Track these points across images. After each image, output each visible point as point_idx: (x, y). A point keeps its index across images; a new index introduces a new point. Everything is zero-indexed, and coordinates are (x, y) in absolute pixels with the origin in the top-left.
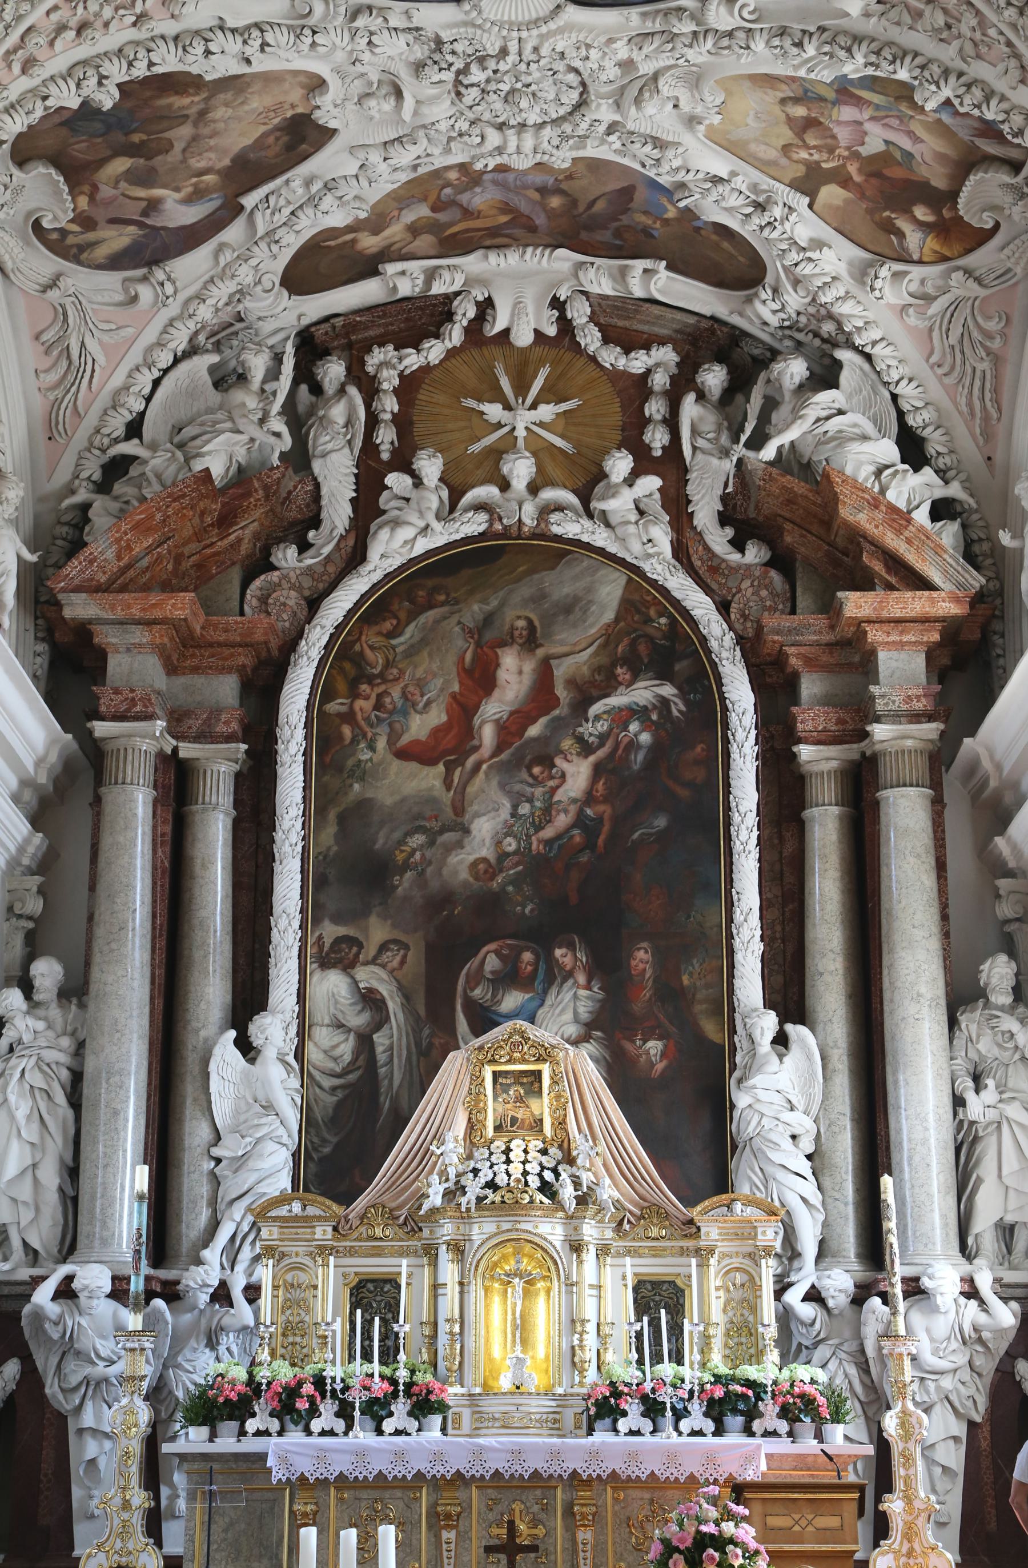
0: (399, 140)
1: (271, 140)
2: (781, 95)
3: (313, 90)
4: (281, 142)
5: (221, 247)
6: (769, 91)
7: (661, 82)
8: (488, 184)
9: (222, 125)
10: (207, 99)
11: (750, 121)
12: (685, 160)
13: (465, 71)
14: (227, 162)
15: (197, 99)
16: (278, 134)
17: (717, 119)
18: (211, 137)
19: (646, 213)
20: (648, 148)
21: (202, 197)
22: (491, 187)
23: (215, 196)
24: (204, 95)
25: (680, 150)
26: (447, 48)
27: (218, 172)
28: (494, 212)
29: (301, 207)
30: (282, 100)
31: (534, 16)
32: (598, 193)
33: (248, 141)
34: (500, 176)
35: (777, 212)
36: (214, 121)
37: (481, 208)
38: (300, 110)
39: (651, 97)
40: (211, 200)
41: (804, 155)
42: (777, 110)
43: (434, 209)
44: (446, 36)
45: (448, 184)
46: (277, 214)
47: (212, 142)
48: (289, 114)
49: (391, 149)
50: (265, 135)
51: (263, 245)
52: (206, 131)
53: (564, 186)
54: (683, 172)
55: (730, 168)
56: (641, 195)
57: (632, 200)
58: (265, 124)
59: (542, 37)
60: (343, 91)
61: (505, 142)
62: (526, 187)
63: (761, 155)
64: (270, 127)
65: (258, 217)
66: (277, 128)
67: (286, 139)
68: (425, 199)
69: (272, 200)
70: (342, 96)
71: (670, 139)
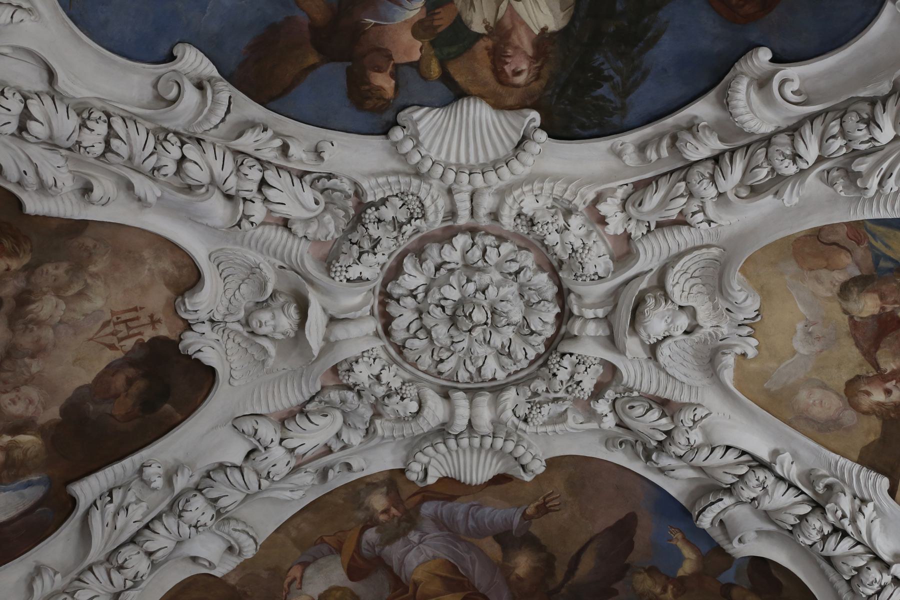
0: (302, 410)
1: (120, 381)
2: (841, 277)
3: (182, 294)
4: (134, 390)
5: (38, 570)
6: (824, 273)
7: (670, 282)
8: (428, 525)
9: (48, 334)
10: (29, 269)
11: (801, 346)
12: (706, 433)
13: (395, 271)
14: (53, 413)
15: (15, 264)
16: (131, 372)
17: (750, 347)
18: (33, 356)
19: (652, 571)
20: (655, 414)
21: (16, 477)
22: (433, 535)
23: (34, 478)
24: (26, 260)
25: (700, 412)
26: (371, 213)
27: (42, 431)
28: (436, 586)
29: (159, 517)
30: (137, 303)
31: (492, 156)
32: (584, 538)
33: (87, 378)
34: (444, 509)
35: (846, 503)
36: (39, 323)
37: (418, 576)
38: (163, 331)
39: (657, 303)
40: (30, 484)
41: (878, 396)
42: (835, 309)
43: (353, 573)
44: (373, 193)
45: (371, 522)
46: (122, 513)
47: (35, 367)
48: (148, 334)
49: (291, 425)
50: (112, 369)
51: (100, 572)
52: (26, 341)
53: (535, 530)
54: (706, 452)
55: (773, 446)
56: (643, 535)
57: (630, 546)
58: (112, 347)
59: (502, 194)
60: (225, 302)
61: (452, 414)
62: (480, 533)
63: (817, 412)
64: (119, 355)
65: (96, 519)
66: (128, 361)
67: (141, 384)
68: (338, 550)
69: (117, 495)
70: (222, 310)
71: (685, 399)
